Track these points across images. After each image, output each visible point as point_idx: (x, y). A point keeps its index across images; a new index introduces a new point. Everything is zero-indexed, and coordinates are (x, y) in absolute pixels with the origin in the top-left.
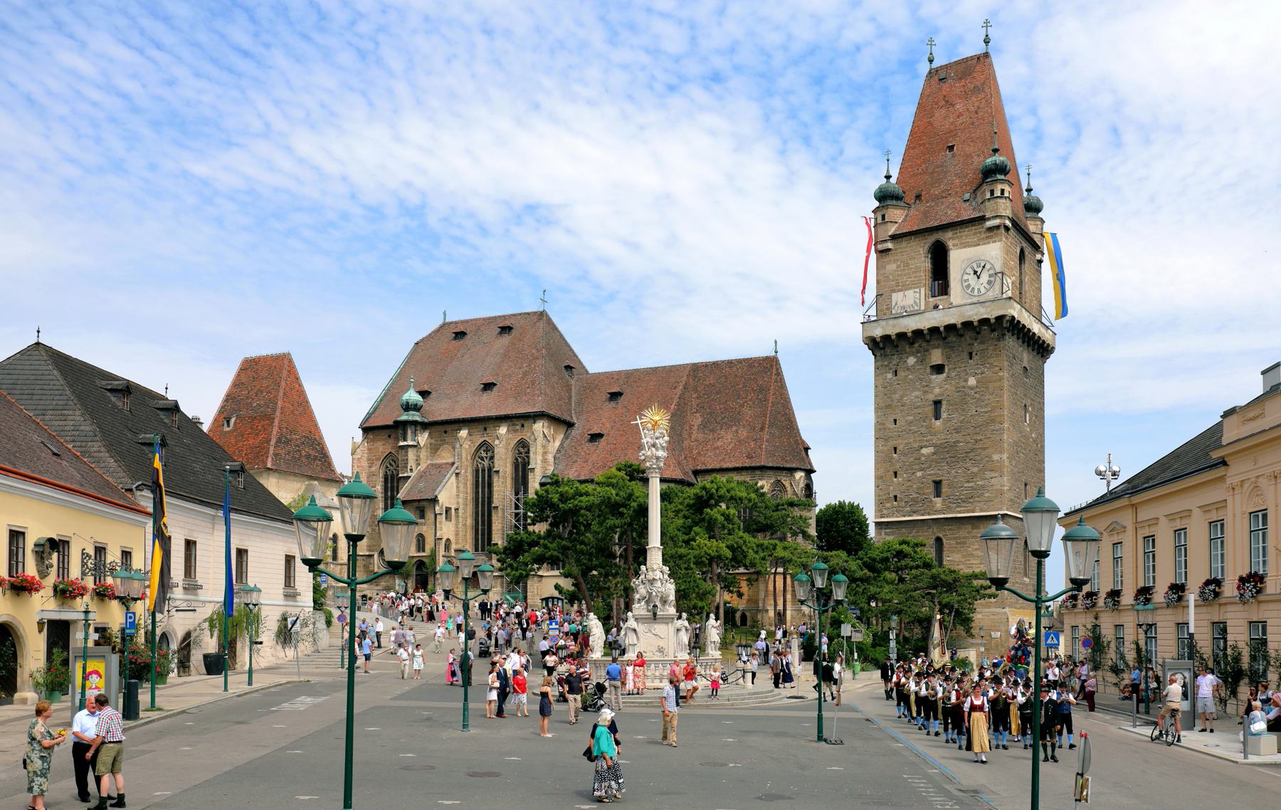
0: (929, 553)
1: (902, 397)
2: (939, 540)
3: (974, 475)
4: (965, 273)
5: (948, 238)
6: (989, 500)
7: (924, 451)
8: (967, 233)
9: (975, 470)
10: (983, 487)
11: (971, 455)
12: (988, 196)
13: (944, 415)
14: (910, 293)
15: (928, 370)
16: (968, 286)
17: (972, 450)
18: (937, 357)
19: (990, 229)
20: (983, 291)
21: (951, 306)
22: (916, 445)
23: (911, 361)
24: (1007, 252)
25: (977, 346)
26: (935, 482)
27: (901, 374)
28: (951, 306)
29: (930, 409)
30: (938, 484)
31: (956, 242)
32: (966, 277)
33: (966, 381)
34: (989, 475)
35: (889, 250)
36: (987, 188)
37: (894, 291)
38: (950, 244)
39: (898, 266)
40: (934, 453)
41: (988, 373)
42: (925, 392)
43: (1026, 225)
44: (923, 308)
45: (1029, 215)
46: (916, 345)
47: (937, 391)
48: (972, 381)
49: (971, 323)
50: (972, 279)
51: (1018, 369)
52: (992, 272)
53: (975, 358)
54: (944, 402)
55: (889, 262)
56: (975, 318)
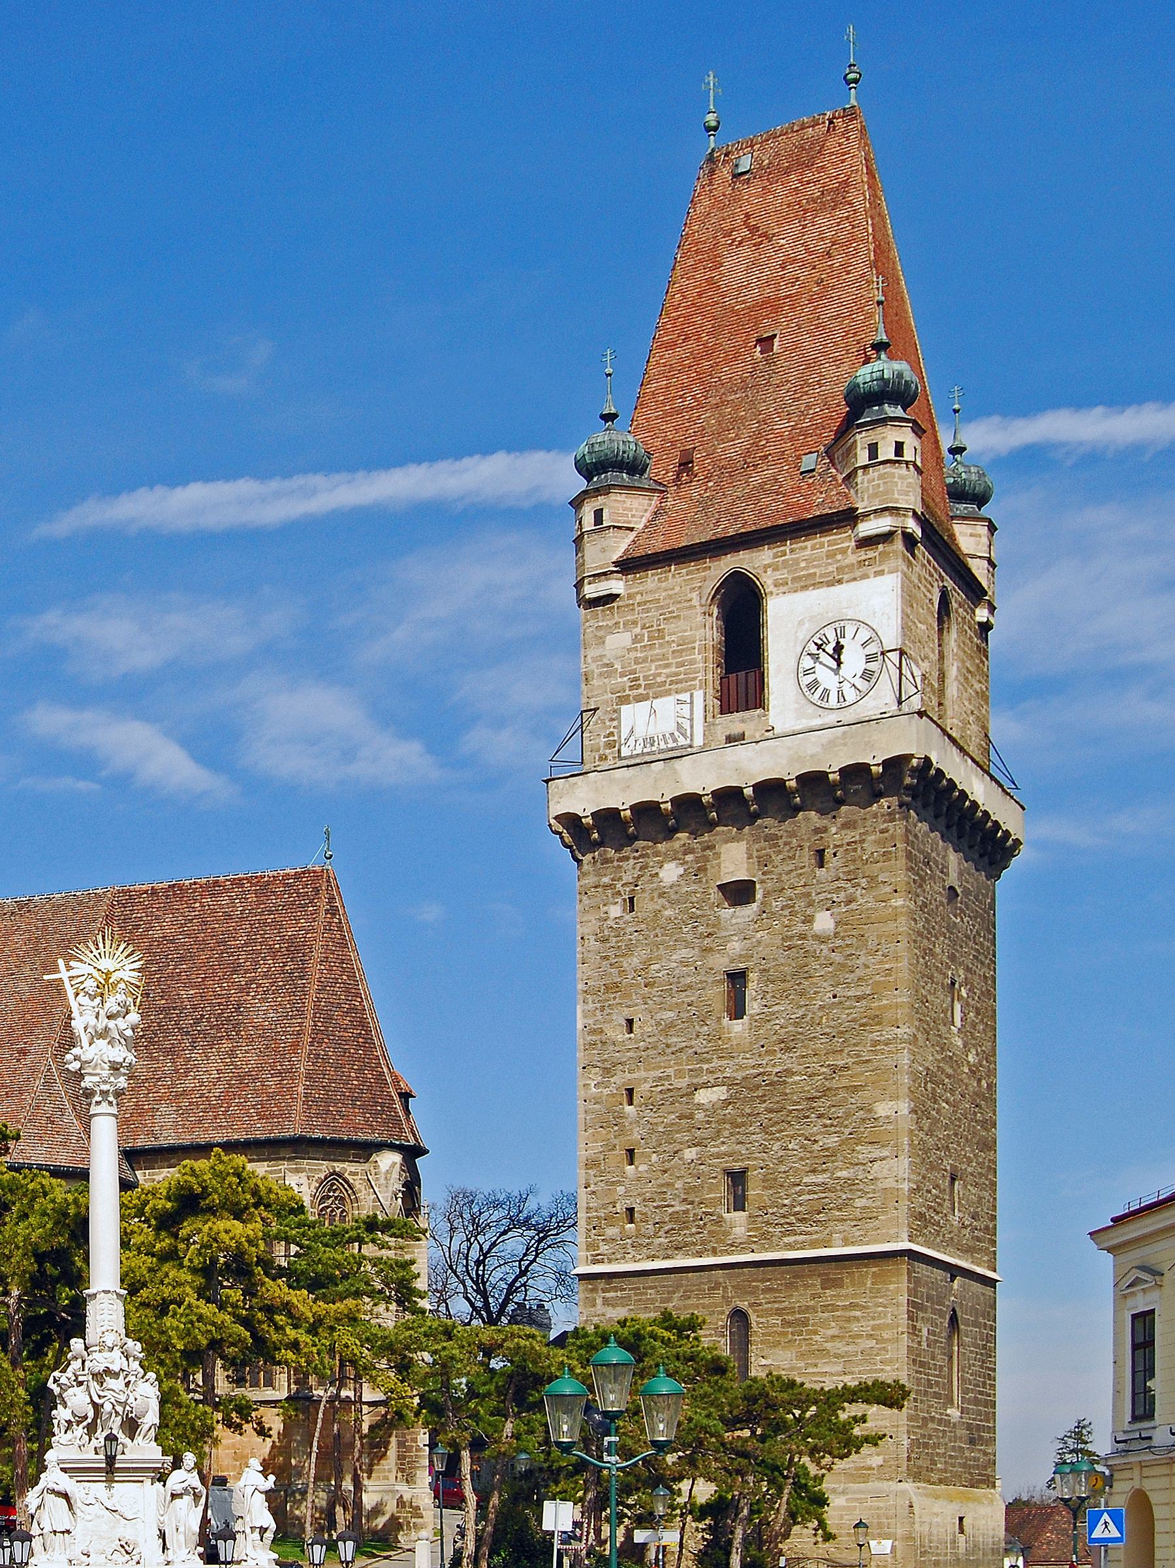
0: (714, 1340)
1: (647, 964)
2: (739, 1317)
3: (830, 1154)
6: (868, 1216)
7: (703, 1097)
9: (832, 1141)
10: (850, 1183)
11: (822, 1105)
13: (753, 1007)
14: (666, 706)
15: (715, 895)
17: (826, 1092)
18: (734, 858)
22: (682, 1083)
23: (670, 873)
24: (909, 598)
25: (835, 835)
26: (729, 1173)
27: (645, 905)
29: (717, 994)
30: (737, 1178)
33: (809, 920)
34: (864, 1152)
35: (612, 598)
36: (862, 440)
37: (624, 700)
39: (636, 639)
40: (727, 1103)
41: (865, 900)
42: (707, 950)
43: (952, 536)
44: (698, 741)
45: (962, 508)
47: (735, 946)
48: (824, 922)
51: (935, 891)
53: (832, 863)
54: (753, 976)
55: (610, 630)
56: (833, 764)
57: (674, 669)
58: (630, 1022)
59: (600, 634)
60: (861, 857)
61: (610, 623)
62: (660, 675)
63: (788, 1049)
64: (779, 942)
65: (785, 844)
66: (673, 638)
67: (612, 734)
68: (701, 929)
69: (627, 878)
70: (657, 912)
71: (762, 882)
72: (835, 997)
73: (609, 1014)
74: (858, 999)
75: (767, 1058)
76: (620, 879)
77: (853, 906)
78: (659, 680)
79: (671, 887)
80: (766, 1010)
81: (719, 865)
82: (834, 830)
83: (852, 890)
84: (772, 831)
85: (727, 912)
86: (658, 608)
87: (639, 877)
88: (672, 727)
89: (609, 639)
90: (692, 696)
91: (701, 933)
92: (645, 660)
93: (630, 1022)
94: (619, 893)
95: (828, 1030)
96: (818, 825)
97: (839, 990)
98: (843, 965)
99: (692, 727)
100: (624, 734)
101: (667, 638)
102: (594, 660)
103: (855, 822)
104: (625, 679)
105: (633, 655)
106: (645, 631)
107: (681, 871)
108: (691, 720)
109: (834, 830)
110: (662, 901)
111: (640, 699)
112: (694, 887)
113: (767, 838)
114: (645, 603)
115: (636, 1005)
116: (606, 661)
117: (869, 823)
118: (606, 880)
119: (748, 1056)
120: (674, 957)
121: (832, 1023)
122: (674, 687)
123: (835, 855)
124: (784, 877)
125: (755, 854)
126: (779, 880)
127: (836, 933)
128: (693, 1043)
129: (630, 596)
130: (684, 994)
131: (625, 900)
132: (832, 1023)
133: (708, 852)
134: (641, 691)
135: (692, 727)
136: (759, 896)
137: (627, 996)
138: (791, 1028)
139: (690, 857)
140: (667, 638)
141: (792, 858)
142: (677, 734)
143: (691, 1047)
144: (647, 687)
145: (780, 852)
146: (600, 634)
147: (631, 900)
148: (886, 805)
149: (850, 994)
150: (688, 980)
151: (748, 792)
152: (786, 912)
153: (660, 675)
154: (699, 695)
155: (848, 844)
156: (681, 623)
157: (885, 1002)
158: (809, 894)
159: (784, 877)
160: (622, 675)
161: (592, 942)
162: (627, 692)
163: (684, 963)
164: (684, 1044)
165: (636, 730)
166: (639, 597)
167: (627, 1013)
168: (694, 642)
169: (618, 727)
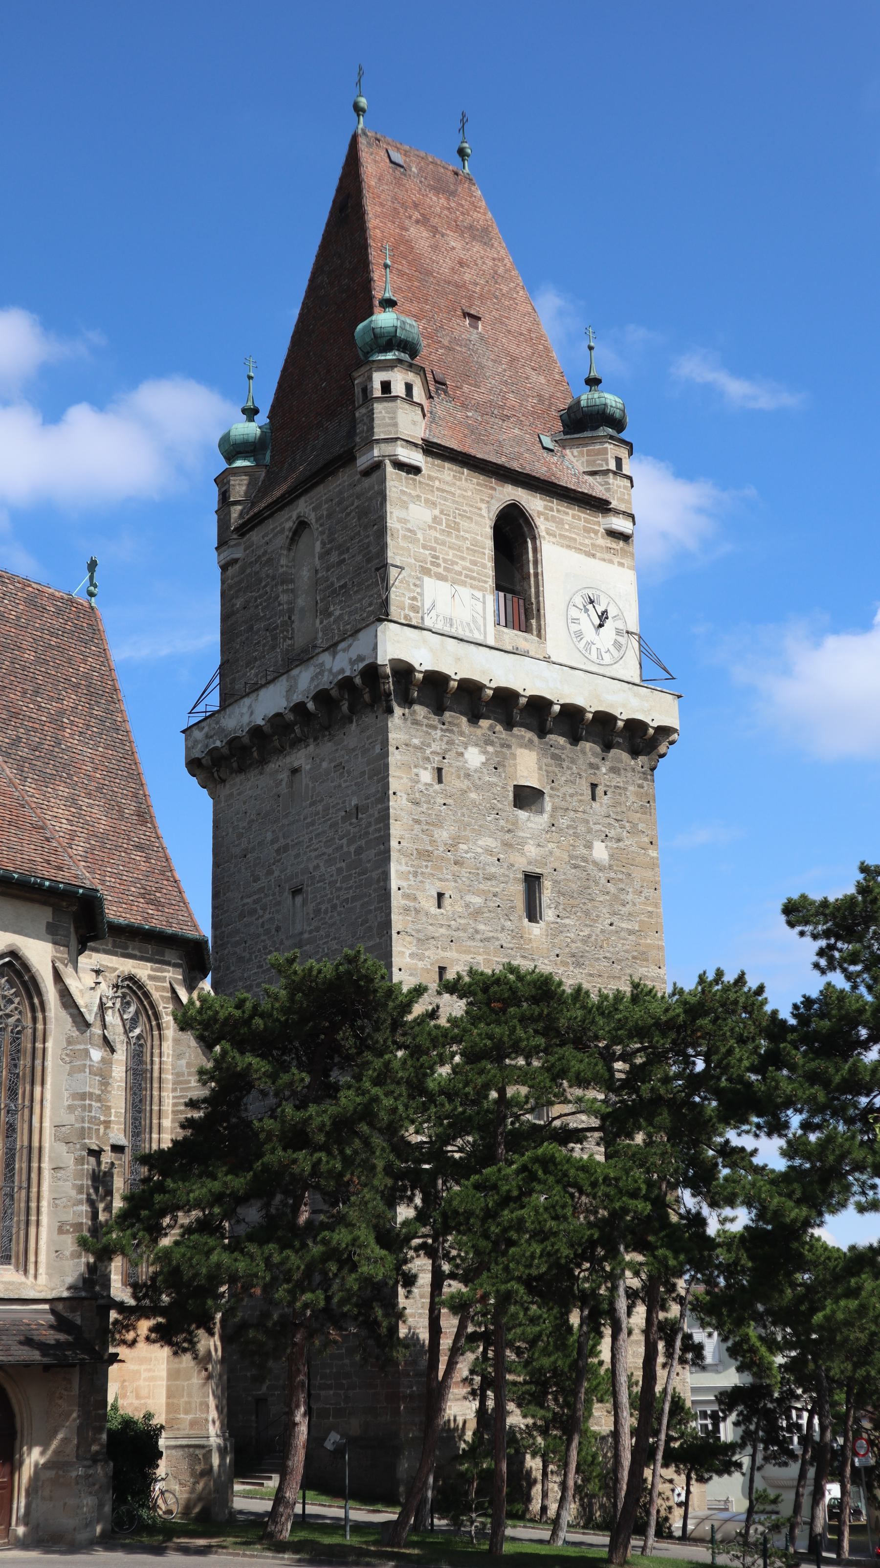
4: (570, 603)
5: (534, 504)
8: (572, 517)
12: (612, 466)
13: (549, 914)
16: (579, 635)
18: (527, 764)
20: (607, 659)
21: (547, 659)
23: (474, 757)
28: (547, 659)
29: (517, 890)
31: (552, 526)
32: (574, 613)
33: (589, 846)
35: (416, 470)
37: (426, 572)
38: (542, 525)
39: (435, 519)
46: (485, 723)
47: (531, 850)
49: (614, 719)
50: (587, 622)
52: (620, 625)
57: (468, 564)
58: (440, 896)
59: (405, 498)
60: (625, 803)
61: (413, 493)
62: (457, 563)
63: (578, 965)
64: (566, 857)
65: (569, 768)
66: (467, 535)
67: (414, 599)
68: (502, 823)
69: (435, 747)
71: (551, 796)
72: (611, 925)
73: (421, 882)
74: (631, 932)
75: (562, 969)
76: (429, 746)
77: (621, 844)
78: (457, 568)
79: (476, 771)
80: (559, 920)
81: (515, 765)
82: (604, 770)
83: (620, 830)
84: (557, 751)
85: (522, 814)
86: (454, 502)
87: (446, 751)
88: (468, 619)
89: (412, 506)
90: (484, 597)
91: (502, 827)
92: (443, 543)
93: (440, 896)
94: (428, 759)
95: (608, 955)
96: (593, 760)
97: (615, 919)
98: (616, 897)
99: (485, 625)
100: (427, 605)
101: (462, 533)
102: (401, 520)
103: (619, 770)
104: (427, 552)
105: (433, 533)
106: (443, 517)
107: (483, 758)
108: (485, 618)
109: (604, 770)
110: (466, 782)
111: (440, 577)
112: (494, 779)
113: (555, 757)
114: (443, 491)
115: (447, 880)
116: (409, 526)
117: (629, 774)
118: (416, 741)
119: (546, 961)
120: (480, 842)
121: (611, 949)
122: (468, 580)
123: (605, 794)
124: (568, 798)
126: (564, 799)
127: (610, 866)
128: (500, 935)
129: (430, 478)
130: (489, 883)
131: (433, 768)
132: (611, 949)
133: (504, 750)
134: (441, 570)
135: (485, 625)
136: (548, 805)
137: (440, 869)
138: (579, 944)
139: (490, 749)
140: (462, 533)
142: (472, 625)
143: (498, 939)
144: (446, 569)
146: (405, 498)
147: (439, 770)
148: (640, 764)
149: (624, 925)
150: (493, 870)
151: (557, 708)
152: (571, 832)
153: (457, 563)
154: (490, 599)
156: (473, 525)
157: (649, 941)
158: (587, 822)
159: (568, 798)
160: (424, 547)
161: (404, 801)
162: (429, 566)
163: (489, 852)
164: (491, 934)
165: (438, 605)
166: (437, 483)
167: (439, 886)
168: (484, 548)
169: (421, 594)
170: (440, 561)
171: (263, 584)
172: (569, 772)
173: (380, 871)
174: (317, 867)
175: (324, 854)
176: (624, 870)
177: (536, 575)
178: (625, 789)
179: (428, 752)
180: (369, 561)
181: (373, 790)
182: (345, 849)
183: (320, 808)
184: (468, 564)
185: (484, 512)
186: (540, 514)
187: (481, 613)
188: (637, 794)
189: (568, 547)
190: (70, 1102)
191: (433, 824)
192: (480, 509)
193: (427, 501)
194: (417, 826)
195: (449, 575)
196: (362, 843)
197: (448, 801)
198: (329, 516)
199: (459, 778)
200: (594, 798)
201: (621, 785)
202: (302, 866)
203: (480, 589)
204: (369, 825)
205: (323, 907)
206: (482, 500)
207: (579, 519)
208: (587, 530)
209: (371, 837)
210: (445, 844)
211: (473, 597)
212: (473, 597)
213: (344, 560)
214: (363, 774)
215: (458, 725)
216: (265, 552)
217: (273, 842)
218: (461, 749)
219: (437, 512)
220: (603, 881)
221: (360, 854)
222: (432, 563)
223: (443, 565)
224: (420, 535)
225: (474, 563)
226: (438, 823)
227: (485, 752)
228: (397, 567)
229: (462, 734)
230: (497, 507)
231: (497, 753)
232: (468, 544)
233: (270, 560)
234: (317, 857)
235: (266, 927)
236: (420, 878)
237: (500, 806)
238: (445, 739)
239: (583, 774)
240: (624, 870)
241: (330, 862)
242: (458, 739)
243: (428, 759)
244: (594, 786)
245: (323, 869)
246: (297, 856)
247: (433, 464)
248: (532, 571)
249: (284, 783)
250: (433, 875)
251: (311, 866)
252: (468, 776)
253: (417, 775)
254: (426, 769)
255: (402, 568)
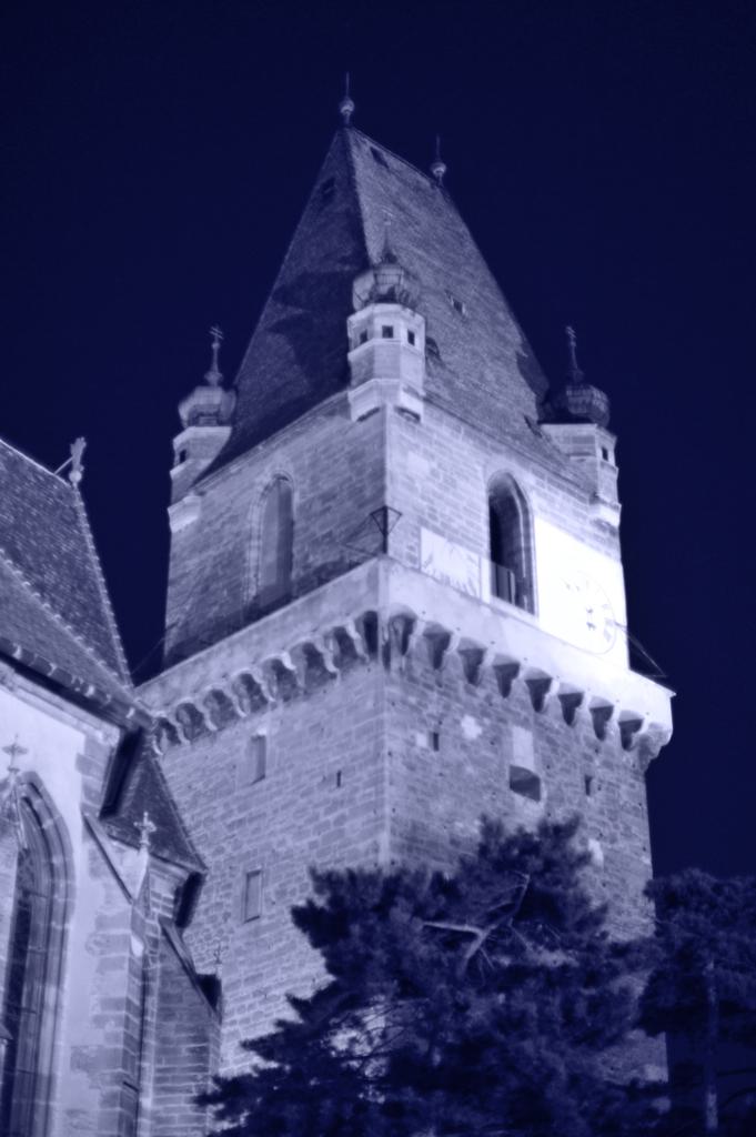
19: (599, 524)
23: (471, 728)
31: (544, 503)
35: (417, 417)
37: (423, 522)
38: (535, 501)
39: (433, 473)
57: (464, 524)
61: (413, 441)
65: (564, 755)
67: (411, 548)
69: (433, 709)
70: (460, 766)
71: (547, 782)
78: (455, 525)
84: (553, 735)
87: (443, 715)
88: (466, 581)
92: (440, 497)
100: (424, 558)
105: (430, 484)
106: (441, 471)
108: (480, 582)
111: (437, 531)
112: (489, 755)
113: (550, 741)
123: (599, 789)
125: (540, 751)
127: (606, 869)
129: (429, 429)
131: (430, 733)
133: (501, 725)
134: (438, 525)
139: (487, 721)
141: (568, 772)
145: (558, 760)
155: (610, 784)
160: (423, 498)
161: (400, 764)
169: (419, 545)
170: (438, 516)
171: (225, 541)
172: (564, 760)
173: (370, 841)
174: (282, 843)
175: (293, 826)
176: (618, 874)
177: (528, 550)
178: (618, 787)
179: (425, 713)
180: (361, 506)
181: (362, 749)
182: (323, 819)
183: (289, 774)
184: (464, 524)
185: (480, 475)
186: (532, 488)
187: (477, 574)
188: (629, 794)
189: (560, 527)
190: (97, 1011)
191: (430, 795)
192: (476, 471)
193: (426, 452)
194: (412, 795)
195: (447, 532)
196: (345, 811)
197: (447, 772)
198: (313, 465)
199: (455, 746)
200: (588, 791)
201: (614, 781)
202: (263, 842)
203: (476, 551)
204: (356, 790)
205: (289, 888)
206: (478, 463)
207: (568, 500)
208: (577, 514)
209: (359, 803)
210: (441, 819)
211: (470, 559)
212: (470, 559)
213: (328, 509)
214: (348, 734)
215: (456, 690)
216: (229, 509)
217: (223, 817)
218: (457, 717)
219: (434, 465)
220: (599, 884)
221: (342, 824)
222: (430, 516)
223: (440, 519)
224: (417, 485)
225: (469, 523)
226: (435, 793)
227: (481, 724)
228: (395, 511)
229: (458, 700)
230: (491, 471)
231: (494, 728)
232: (464, 504)
233: (234, 519)
234: (282, 831)
235: (211, 914)
236: (415, 853)
237: (496, 785)
238: (442, 702)
239: (578, 765)
240: (618, 874)
241: (300, 834)
242: (456, 706)
243: (423, 721)
244: (588, 780)
245: (290, 843)
246: (257, 830)
247: (431, 416)
248: (523, 545)
249: (242, 752)
250: (428, 852)
251: (274, 840)
252: (464, 747)
253: (413, 737)
254: (421, 732)
255: (400, 514)
